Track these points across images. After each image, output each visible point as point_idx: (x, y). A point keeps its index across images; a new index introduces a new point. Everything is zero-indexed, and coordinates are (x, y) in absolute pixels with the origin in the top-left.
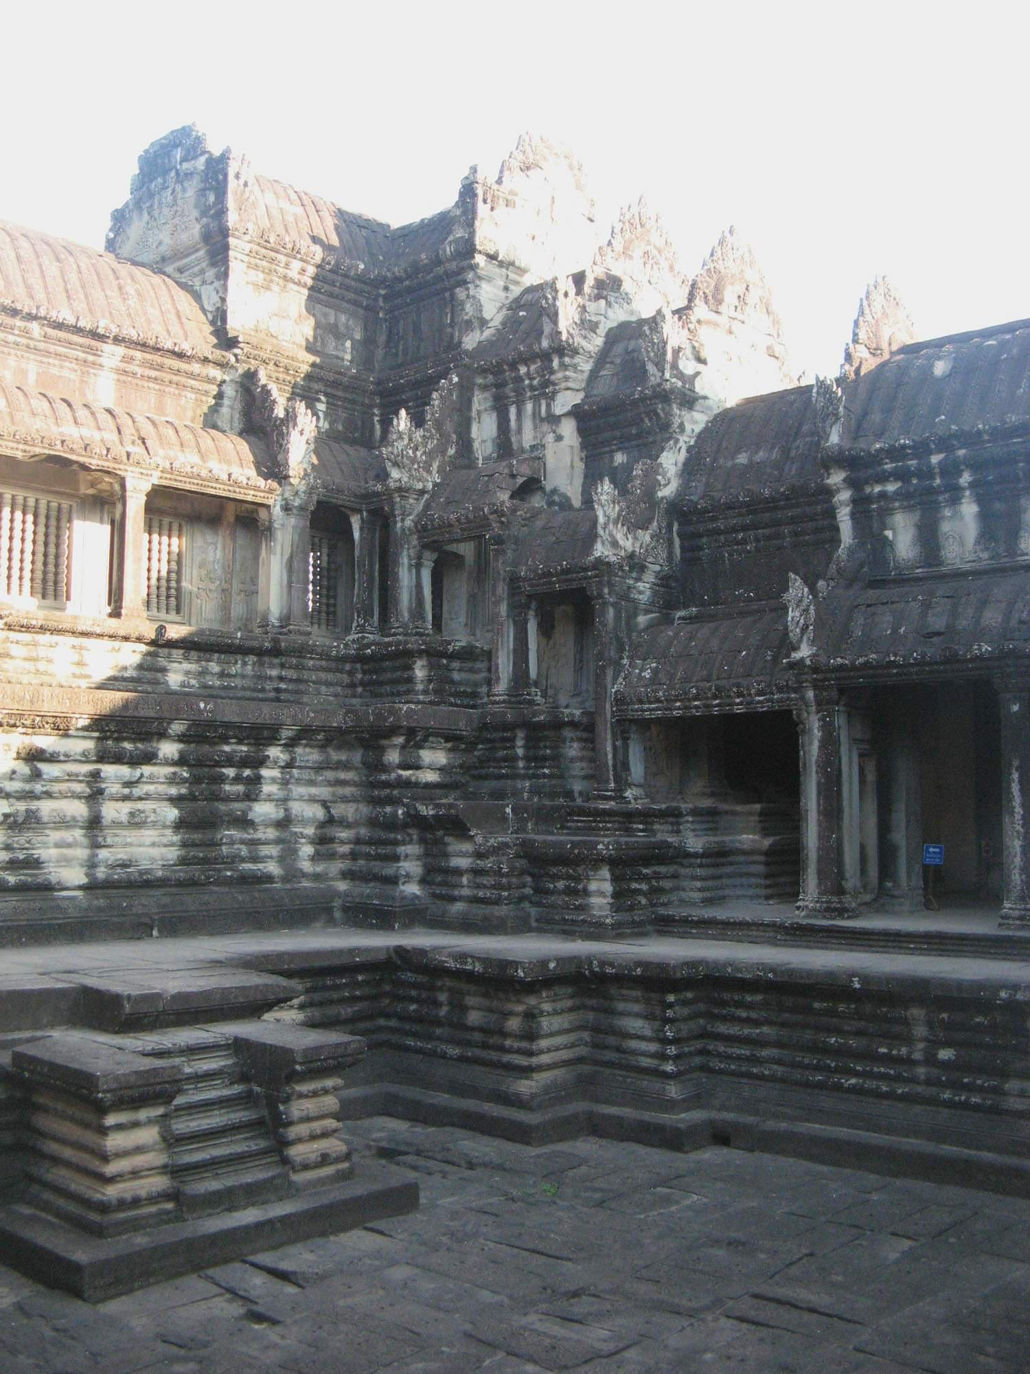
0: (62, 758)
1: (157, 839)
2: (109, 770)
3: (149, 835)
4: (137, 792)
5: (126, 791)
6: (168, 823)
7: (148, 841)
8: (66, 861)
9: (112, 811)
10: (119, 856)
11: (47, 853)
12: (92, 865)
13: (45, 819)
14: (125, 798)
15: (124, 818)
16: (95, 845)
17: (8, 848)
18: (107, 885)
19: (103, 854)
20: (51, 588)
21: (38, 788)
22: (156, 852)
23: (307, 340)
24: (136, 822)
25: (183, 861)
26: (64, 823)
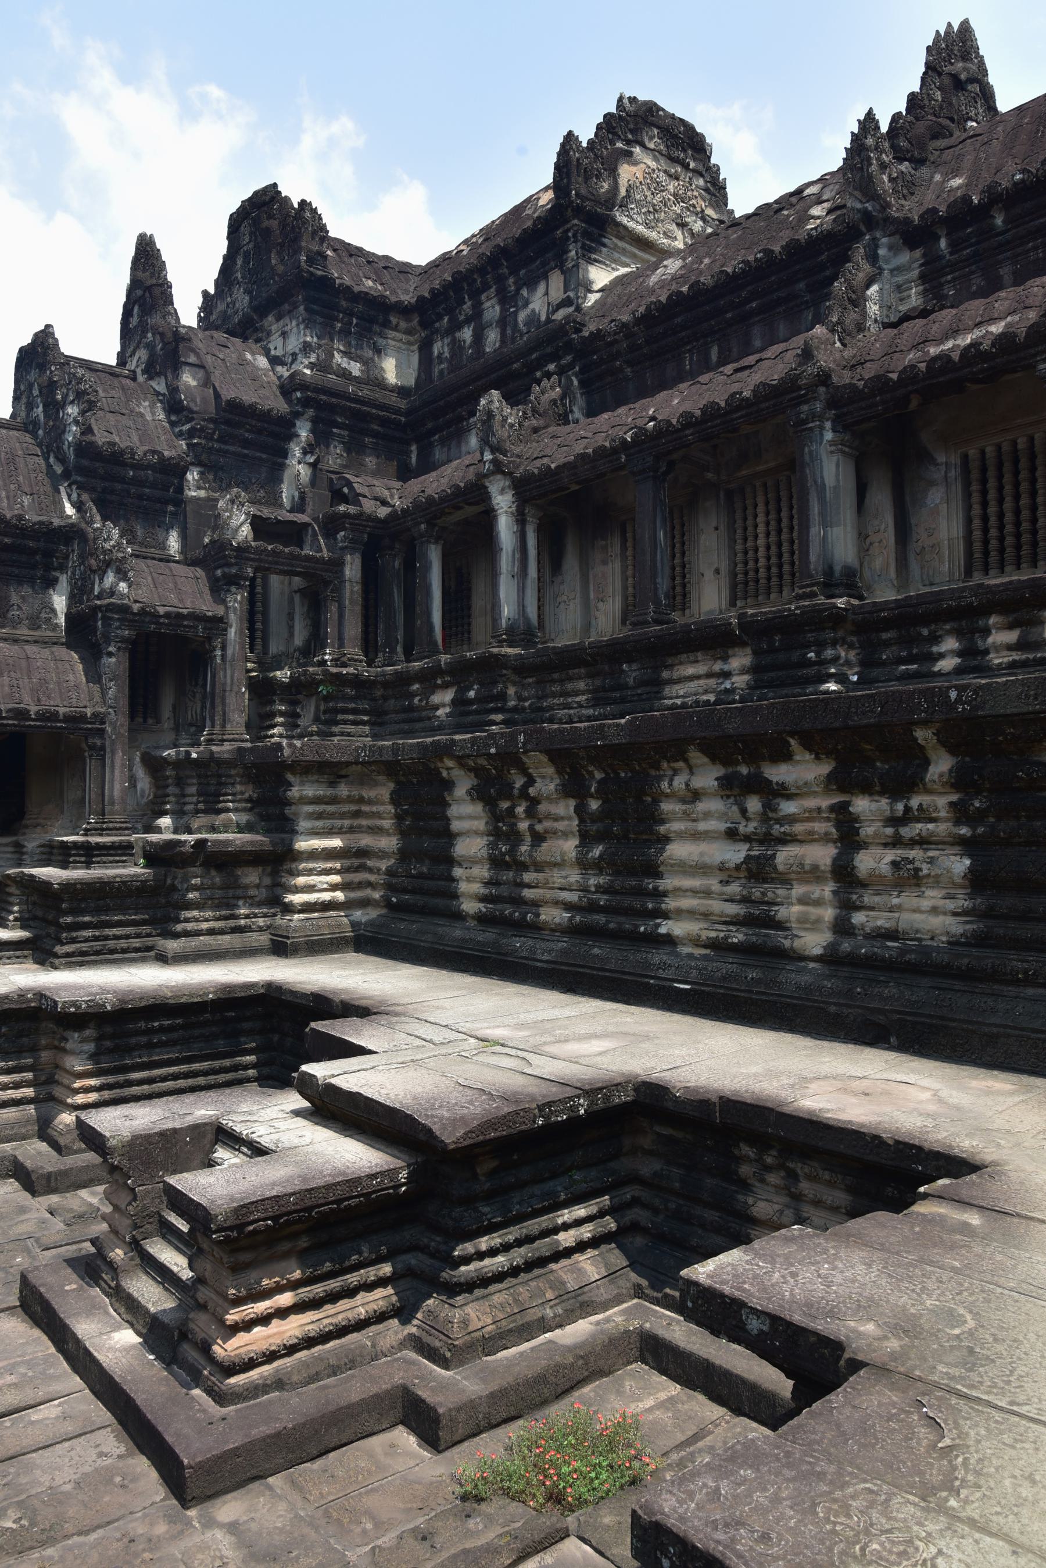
0: (793, 790)
1: (941, 903)
2: (861, 805)
3: (933, 897)
4: (906, 832)
5: (889, 831)
6: (958, 880)
7: (926, 904)
8: (814, 925)
9: (866, 862)
10: (879, 923)
11: (791, 912)
12: (842, 927)
13: (781, 868)
14: (896, 842)
15: (885, 868)
16: (847, 906)
17: (745, 900)
18: (853, 961)
19: (858, 918)
20: (1026, 550)
21: (777, 829)
22: (937, 922)
23: (949, 25)
24: (907, 877)
25: (978, 941)
26: (813, 874)
